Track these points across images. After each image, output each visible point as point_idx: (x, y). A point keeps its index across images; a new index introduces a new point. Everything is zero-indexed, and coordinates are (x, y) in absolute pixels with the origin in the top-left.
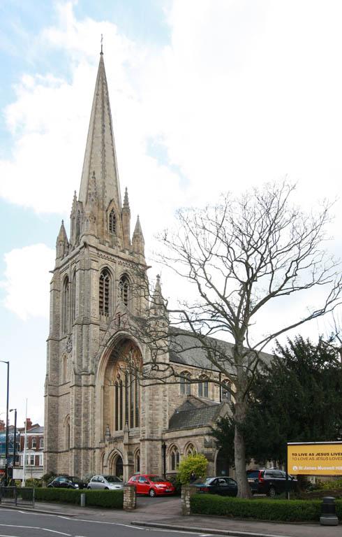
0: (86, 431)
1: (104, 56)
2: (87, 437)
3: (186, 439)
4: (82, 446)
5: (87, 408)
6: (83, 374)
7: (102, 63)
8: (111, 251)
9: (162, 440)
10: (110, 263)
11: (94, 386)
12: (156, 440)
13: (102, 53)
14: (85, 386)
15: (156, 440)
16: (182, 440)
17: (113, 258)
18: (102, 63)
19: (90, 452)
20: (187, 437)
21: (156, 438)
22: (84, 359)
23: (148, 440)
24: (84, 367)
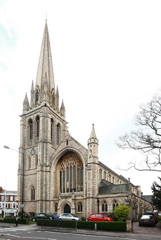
0: (46, 193)
1: (47, 22)
2: (46, 195)
3: (112, 198)
4: (44, 199)
5: (46, 182)
6: (44, 166)
7: (46, 25)
8: (54, 111)
9: (97, 198)
10: (54, 117)
11: (50, 172)
12: (95, 198)
13: (46, 20)
14: (45, 171)
15: (95, 198)
16: (110, 198)
17: (55, 115)
18: (46, 25)
19: (48, 203)
20: (113, 197)
21: (94, 197)
22: (45, 159)
23: (92, 198)
24: (44, 163)
